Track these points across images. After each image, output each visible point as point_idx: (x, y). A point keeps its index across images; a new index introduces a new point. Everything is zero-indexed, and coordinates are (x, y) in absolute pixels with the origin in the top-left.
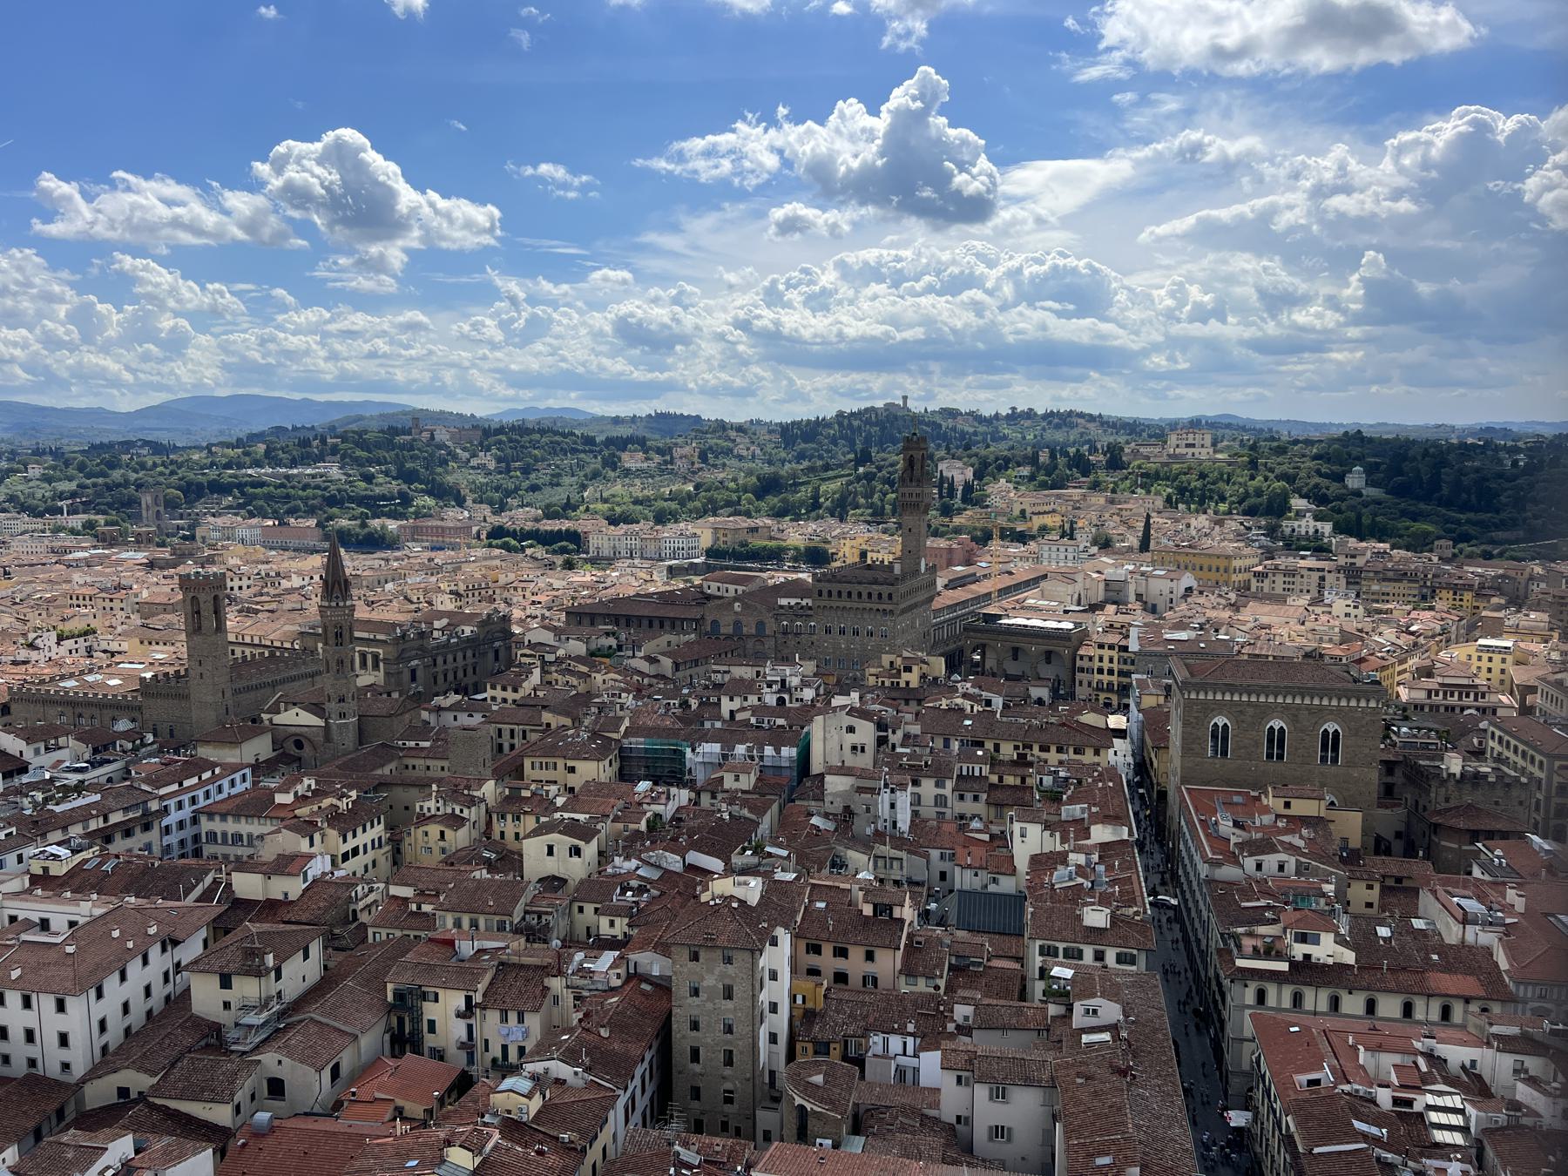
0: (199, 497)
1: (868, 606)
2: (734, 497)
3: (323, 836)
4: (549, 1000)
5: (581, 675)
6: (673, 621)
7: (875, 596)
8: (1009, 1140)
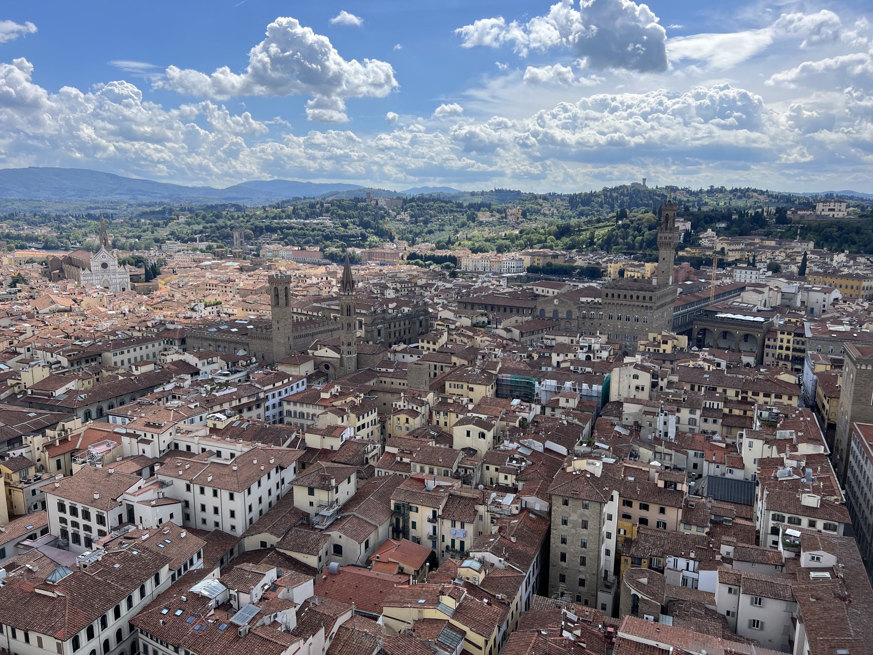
0: (261, 234)
1: (637, 303)
2: (543, 238)
4: (477, 517)
5: (469, 337)
6: (518, 309)
7: (641, 298)
8: (762, 629)
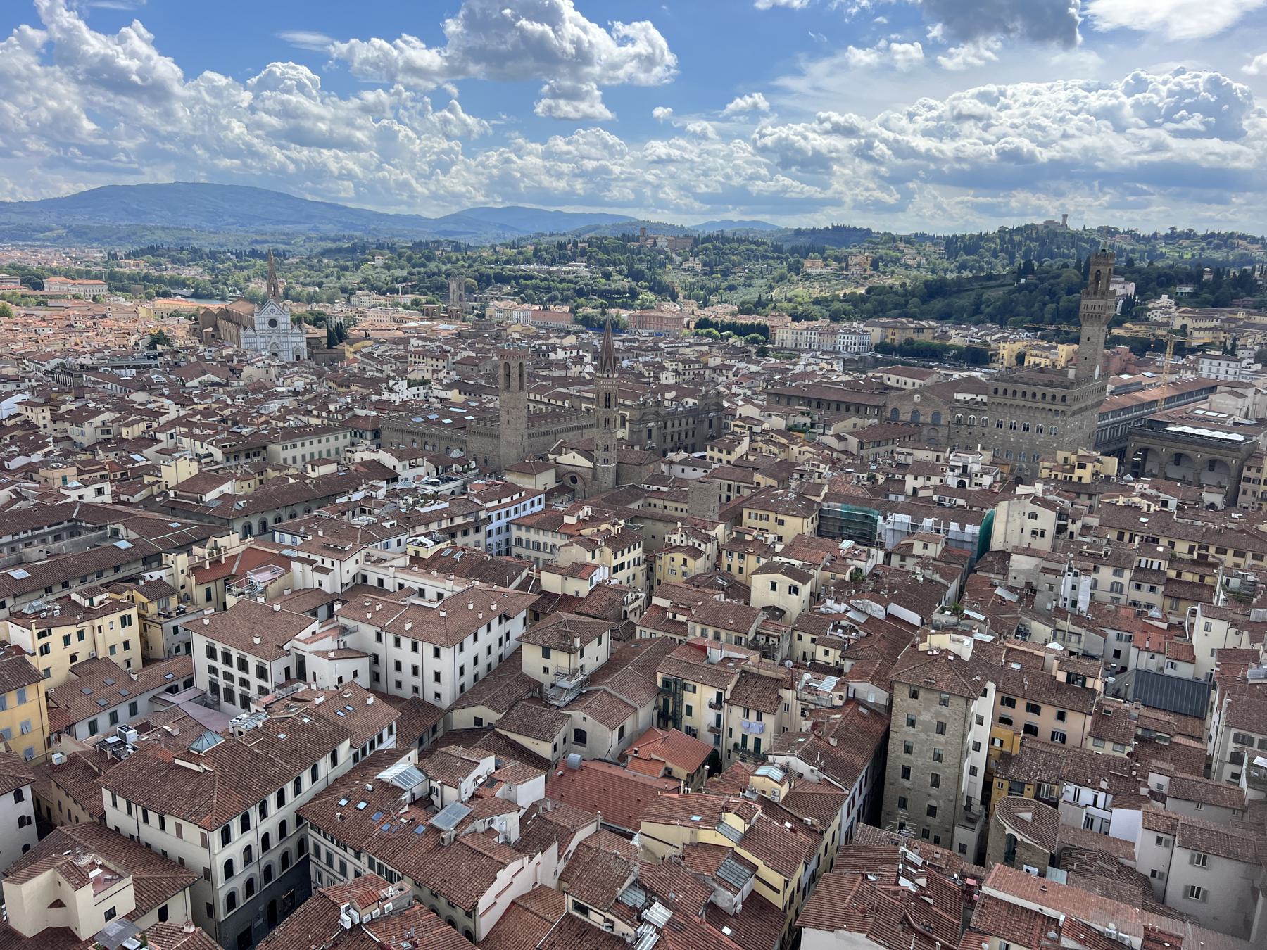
0: (488, 284)
3: (601, 552)
4: (782, 706)
5: (781, 446)
6: (858, 406)
7: (1049, 398)
8: (1204, 900)
